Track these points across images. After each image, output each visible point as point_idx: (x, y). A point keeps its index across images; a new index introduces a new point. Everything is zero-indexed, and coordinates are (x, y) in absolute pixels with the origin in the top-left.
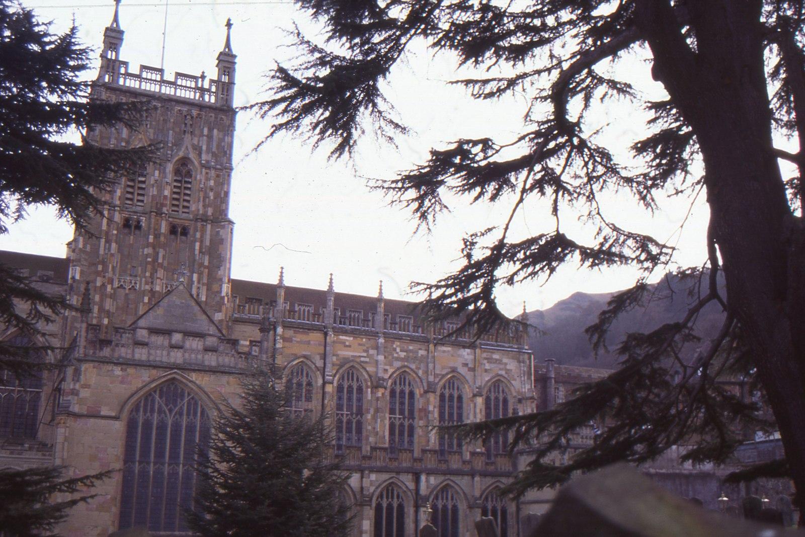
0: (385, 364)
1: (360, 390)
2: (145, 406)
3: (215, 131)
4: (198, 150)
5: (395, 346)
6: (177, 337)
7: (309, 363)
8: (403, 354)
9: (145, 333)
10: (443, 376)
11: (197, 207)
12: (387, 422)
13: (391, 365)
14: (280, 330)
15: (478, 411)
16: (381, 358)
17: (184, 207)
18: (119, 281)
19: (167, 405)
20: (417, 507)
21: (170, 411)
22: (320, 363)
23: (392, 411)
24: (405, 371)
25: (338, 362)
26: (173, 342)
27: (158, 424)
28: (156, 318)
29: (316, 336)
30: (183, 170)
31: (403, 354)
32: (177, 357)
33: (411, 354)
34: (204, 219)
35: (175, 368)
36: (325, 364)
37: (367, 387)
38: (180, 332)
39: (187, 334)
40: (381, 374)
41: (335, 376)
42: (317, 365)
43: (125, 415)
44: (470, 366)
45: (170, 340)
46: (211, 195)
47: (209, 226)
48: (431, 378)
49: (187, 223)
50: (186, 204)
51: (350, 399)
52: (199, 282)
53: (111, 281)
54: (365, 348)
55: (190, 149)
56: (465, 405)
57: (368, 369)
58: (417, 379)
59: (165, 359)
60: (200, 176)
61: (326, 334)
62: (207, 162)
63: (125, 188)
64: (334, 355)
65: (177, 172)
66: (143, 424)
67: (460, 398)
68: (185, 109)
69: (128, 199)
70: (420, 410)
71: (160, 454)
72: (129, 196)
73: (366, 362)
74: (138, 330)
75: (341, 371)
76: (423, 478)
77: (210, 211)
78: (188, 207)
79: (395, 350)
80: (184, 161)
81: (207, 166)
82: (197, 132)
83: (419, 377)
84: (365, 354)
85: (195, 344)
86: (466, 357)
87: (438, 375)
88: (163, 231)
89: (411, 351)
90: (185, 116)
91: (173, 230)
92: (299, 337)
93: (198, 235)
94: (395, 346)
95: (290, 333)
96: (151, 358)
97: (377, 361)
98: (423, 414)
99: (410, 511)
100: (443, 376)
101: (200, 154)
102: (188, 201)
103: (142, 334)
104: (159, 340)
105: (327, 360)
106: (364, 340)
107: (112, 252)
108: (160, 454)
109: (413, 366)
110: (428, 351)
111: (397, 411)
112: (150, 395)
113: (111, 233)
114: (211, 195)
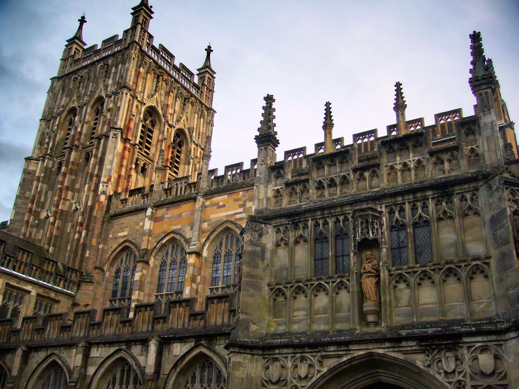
3: (120, 66)
4: (106, 86)
7: (178, 237)
14: (149, 211)
47: (102, 141)
54: (241, 203)
61: (195, 199)
76: (153, 347)
84: (241, 210)
88: (71, 160)
95: (161, 212)
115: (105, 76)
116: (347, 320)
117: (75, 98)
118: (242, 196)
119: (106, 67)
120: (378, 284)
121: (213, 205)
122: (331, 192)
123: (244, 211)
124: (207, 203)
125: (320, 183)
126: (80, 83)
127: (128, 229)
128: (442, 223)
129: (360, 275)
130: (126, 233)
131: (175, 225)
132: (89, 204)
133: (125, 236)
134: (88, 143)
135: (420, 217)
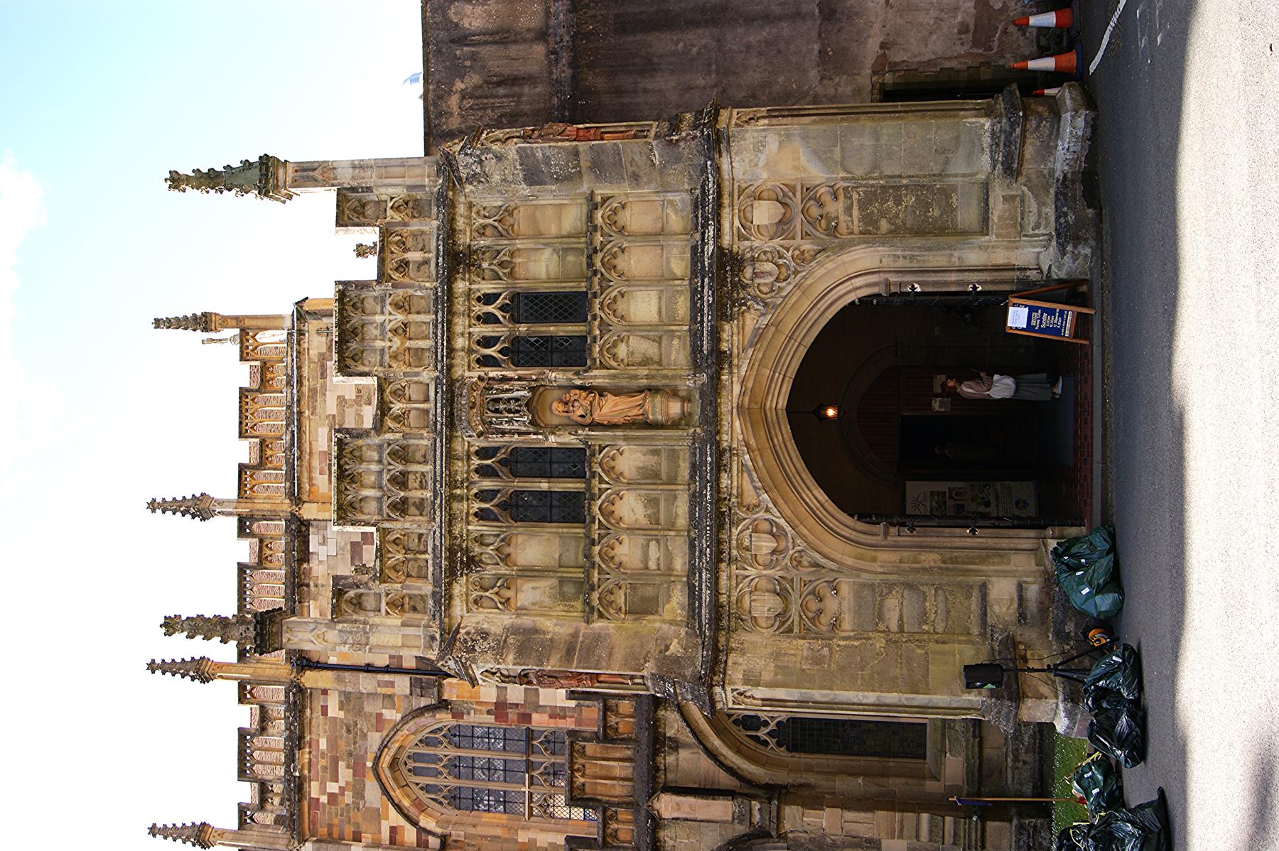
5: (324, 799)
8: (345, 774)
13: (377, 816)
24: (394, 764)
33: (342, 743)
48: (402, 684)
58: (412, 725)
79: (332, 797)
83: (405, 719)
86: (331, 549)
89: (333, 743)
94: (324, 799)
109: (375, 739)
111: (510, 787)
116: (673, 455)
120: (617, 392)
122: (417, 485)
125: (393, 506)
128: (520, 272)
129: (594, 425)
135: (501, 308)
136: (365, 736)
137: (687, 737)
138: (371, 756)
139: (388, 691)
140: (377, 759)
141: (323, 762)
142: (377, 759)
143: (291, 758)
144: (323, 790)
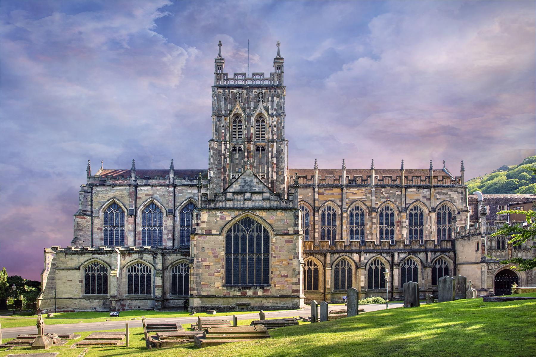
0: (376, 201)
1: (363, 215)
2: (235, 228)
5: (381, 192)
6: (248, 195)
8: (386, 195)
9: (231, 194)
10: (411, 203)
11: (269, 136)
12: (378, 229)
13: (380, 201)
14: (316, 190)
15: (433, 220)
16: (374, 198)
17: (262, 137)
18: (233, 175)
19: (245, 228)
20: (392, 271)
21: (248, 230)
22: (340, 203)
23: (381, 223)
25: (350, 202)
26: (246, 197)
27: (241, 237)
28: (236, 187)
29: (337, 191)
30: (260, 119)
31: (386, 195)
32: (249, 204)
34: (272, 141)
35: (247, 210)
36: (342, 203)
37: (367, 213)
38: (249, 192)
39: (253, 193)
40: (374, 206)
41: (348, 209)
42: (338, 204)
43: (224, 233)
44: (427, 197)
45: (244, 197)
46: (275, 129)
47: (275, 144)
48: (404, 206)
49: (264, 144)
50: (263, 136)
51: (357, 219)
52: (272, 172)
53: (228, 176)
54: (364, 194)
55: (263, 109)
56: (424, 218)
57: (366, 204)
59: (242, 206)
60: (269, 120)
61: (342, 189)
62: (272, 114)
63: (231, 133)
64: (347, 199)
65: (257, 121)
66: (234, 237)
67: (422, 214)
68: (258, 90)
69: (233, 138)
70: (397, 222)
71: (244, 250)
72: (234, 136)
73: (365, 201)
74: (227, 193)
75: (352, 206)
77: (275, 137)
78: (264, 137)
80: (260, 116)
81: (272, 116)
82: (266, 100)
83: (397, 206)
84: (365, 197)
85: (256, 197)
87: (408, 204)
88: (252, 149)
90: (259, 93)
91: (258, 149)
92: (327, 192)
93: (270, 149)
95: (321, 191)
96: (235, 206)
97: (371, 200)
98: (399, 224)
99: (388, 272)
100: (411, 203)
101: (268, 111)
102: (264, 134)
103: (229, 195)
104: (239, 197)
105: (343, 201)
106: (364, 190)
107: (228, 162)
108: (244, 250)
109: (393, 200)
110: (401, 192)
112: (236, 223)
113: (226, 154)
114: (275, 129)
115: (262, 101)
117: (238, 107)
118: (365, 191)
119: (261, 93)
121: (350, 192)
123: (366, 198)
124: (348, 191)
126: (239, 98)
127: (302, 195)
130: (301, 197)
131: (331, 198)
132: (275, 178)
133: (301, 199)
134: (255, 140)
136: (393, 199)
137: (436, 256)
138: (390, 200)
139: (403, 203)
140: (390, 201)
141: (388, 191)
142: (390, 201)
143: (389, 186)
144: (383, 191)
